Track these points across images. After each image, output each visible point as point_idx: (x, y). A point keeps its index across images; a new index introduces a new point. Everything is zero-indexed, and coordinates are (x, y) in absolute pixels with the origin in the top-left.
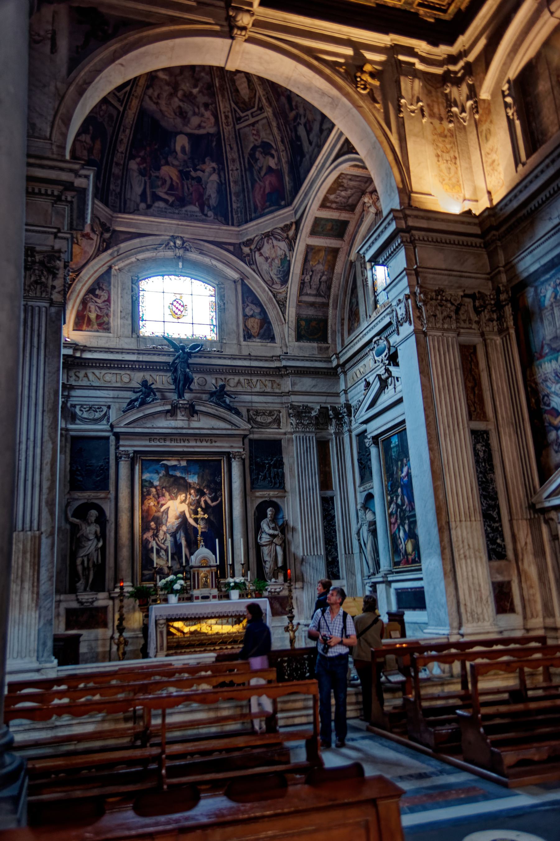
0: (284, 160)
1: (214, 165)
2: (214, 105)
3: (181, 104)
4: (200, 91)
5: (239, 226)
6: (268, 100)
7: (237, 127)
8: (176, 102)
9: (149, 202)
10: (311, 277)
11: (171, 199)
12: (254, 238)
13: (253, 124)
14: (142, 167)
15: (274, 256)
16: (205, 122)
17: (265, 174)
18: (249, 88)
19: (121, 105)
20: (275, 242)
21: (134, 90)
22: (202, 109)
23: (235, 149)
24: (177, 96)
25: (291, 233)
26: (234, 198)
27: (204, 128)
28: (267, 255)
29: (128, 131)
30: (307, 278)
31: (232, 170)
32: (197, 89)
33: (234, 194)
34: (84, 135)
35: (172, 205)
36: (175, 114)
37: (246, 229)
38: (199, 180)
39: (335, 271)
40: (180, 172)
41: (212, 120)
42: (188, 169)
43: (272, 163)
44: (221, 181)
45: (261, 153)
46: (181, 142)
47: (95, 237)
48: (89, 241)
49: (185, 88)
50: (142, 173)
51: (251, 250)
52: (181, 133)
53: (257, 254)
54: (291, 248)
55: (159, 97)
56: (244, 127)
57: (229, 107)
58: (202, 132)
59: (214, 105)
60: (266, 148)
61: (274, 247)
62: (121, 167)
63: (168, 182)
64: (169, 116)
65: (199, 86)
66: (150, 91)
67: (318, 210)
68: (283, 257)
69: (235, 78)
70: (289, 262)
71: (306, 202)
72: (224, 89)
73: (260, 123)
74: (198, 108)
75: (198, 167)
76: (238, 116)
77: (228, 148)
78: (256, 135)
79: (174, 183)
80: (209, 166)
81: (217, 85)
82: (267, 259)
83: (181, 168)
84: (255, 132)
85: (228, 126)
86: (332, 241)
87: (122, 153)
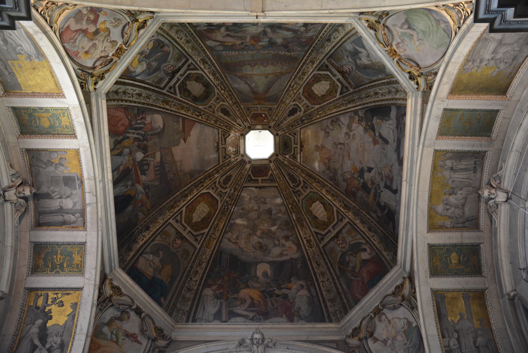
0: (376, 243)
1: (301, 282)
2: (294, 236)
3: (260, 240)
4: (278, 228)
5: (338, 321)
6: (346, 207)
7: (321, 246)
8: (255, 239)
9: (224, 318)
10: (458, 339)
11: (251, 315)
12: (361, 323)
13: (337, 236)
14: (217, 292)
15: (393, 333)
16: (287, 251)
17: (361, 268)
18: (326, 209)
19: (199, 244)
20: (390, 314)
21: (211, 232)
22: (283, 241)
23: (322, 262)
24: (256, 234)
25: (406, 291)
26: (329, 304)
27: (287, 255)
28: (384, 337)
29: (204, 265)
30: (453, 342)
31: (322, 281)
32: (276, 227)
33: (329, 300)
34: (151, 256)
35: (252, 319)
36: (255, 248)
37: (348, 321)
38: (285, 296)
39: (494, 327)
40: (263, 292)
41: (295, 247)
42: (271, 289)
43: (365, 256)
44: (312, 295)
45: (352, 255)
46: (262, 269)
47: (145, 342)
48: (136, 344)
49: (263, 228)
50: (217, 297)
51: (360, 340)
52: (262, 262)
53: (370, 342)
54: (413, 308)
55: (237, 238)
56: (328, 242)
57: (309, 232)
58: (284, 258)
59: (294, 236)
60: (356, 249)
61: (389, 321)
62: (194, 292)
63: (249, 301)
64: (248, 251)
65: (278, 224)
66: (229, 234)
67: (428, 232)
68: (406, 327)
69: (311, 209)
70: (418, 328)
71: (410, 234)
72: (302, 220)
73: (343, 231)
74: (279, 241)
75: (282, 287)
76: (320, 237)
77: (315, 265)
78: (342, 244)
79: (255, 302)
80: (295, 284)
81: (295, 218)
82: (385, 342)
83: (263, 289)
84: (341, 242)
85: (311, 248)
86: (467, 279)
87: (196, 281)
